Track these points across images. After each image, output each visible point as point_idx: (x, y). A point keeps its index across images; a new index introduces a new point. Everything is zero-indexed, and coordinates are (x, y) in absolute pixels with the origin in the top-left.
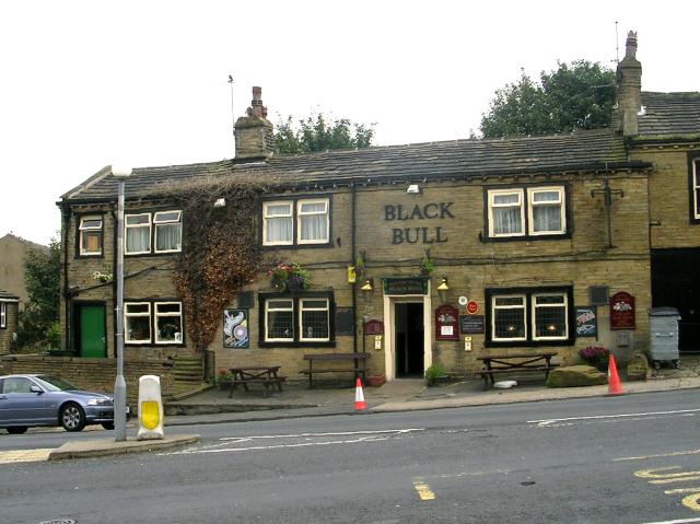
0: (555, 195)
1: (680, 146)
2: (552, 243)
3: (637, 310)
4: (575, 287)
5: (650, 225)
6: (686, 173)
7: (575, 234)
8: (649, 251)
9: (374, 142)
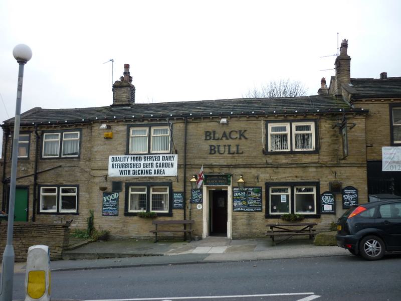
0: (308, 128)
1: (385, 100)
2: (307, 156)
3: (359, 197)
4: (321, 183)
5: (367, 146)
6: (388, 117)
7: (320, 151)
8: (366, 162)
9: (388, 76)
